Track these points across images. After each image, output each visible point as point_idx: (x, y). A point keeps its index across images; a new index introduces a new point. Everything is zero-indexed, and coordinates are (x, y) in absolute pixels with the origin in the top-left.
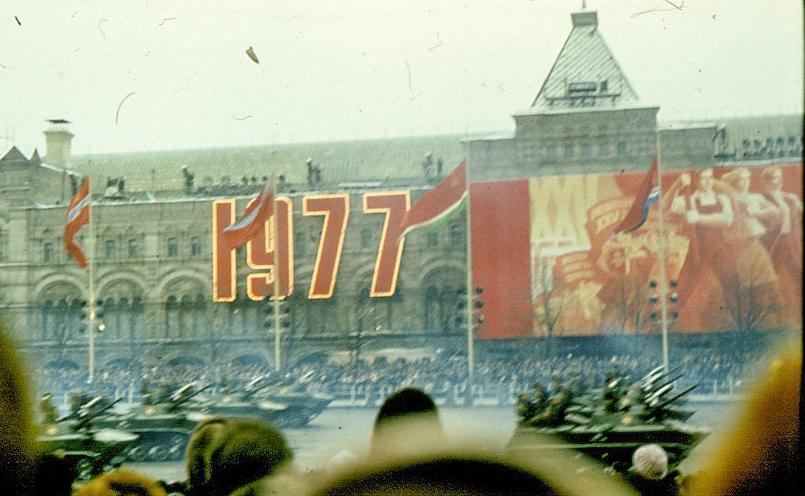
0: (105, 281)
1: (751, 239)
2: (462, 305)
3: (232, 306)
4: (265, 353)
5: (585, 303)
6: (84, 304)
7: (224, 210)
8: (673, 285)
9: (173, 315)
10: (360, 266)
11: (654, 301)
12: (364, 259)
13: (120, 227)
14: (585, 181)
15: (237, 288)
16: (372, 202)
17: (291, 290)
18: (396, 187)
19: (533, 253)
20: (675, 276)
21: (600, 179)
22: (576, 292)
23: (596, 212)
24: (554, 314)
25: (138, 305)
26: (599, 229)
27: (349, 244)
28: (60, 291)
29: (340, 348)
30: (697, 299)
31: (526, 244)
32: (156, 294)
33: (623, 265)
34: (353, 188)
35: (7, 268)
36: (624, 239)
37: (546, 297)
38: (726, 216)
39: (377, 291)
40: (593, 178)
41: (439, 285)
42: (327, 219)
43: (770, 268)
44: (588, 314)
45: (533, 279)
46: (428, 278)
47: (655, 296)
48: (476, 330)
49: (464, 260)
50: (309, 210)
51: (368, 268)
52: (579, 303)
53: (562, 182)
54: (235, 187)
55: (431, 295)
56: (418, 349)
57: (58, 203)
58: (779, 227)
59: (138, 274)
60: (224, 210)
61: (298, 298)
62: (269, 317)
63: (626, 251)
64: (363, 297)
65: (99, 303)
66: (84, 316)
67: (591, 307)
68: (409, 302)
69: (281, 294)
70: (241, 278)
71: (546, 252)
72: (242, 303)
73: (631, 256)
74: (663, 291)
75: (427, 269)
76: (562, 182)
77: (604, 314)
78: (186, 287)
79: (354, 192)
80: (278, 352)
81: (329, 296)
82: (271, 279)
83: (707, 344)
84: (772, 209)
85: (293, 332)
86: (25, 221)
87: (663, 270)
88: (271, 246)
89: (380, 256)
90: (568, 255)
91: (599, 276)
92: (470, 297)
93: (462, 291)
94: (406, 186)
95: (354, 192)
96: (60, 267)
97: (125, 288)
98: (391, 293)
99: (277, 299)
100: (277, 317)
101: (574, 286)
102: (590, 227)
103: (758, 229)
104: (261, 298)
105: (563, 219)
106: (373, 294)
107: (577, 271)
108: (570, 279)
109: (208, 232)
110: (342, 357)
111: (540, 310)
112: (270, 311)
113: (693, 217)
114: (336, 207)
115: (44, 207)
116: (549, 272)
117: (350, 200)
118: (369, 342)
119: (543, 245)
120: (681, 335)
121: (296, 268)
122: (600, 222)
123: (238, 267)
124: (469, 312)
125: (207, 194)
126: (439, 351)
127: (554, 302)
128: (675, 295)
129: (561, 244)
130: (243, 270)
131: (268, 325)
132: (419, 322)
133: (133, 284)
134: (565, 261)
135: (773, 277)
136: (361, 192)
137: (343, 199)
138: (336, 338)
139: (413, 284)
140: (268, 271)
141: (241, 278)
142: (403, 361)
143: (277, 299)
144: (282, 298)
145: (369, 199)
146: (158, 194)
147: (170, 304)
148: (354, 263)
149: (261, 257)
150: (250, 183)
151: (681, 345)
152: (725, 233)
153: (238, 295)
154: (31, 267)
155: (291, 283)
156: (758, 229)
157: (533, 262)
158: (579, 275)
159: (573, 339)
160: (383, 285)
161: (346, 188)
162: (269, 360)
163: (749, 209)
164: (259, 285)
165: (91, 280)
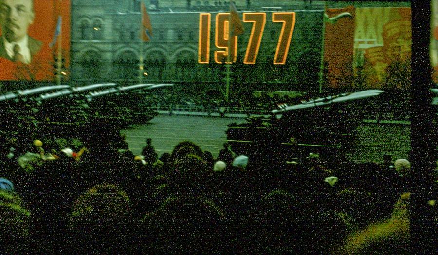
0: (149, 51)
2: (318, 70)
4: (220, 88)
6: (138, 62)
7: (205, 18)
9: (179, 69)
10: (269, 49)
12: (271, 46)
13: (155, 25)
14: (383, 11)
15: (210, 58)
16: (278, 17)
17: (235, 59)
18: (290, 9)
19: (355, 47)
21: (392, 11)
23: (387, 27)
25: (163, 64)
26: (389, 34)
28: (128, 55)
32: (172, 58)
34: (268, 9)
35: (101, 43)
36: (401, 42)
37: (359, 68)
40: (388, 9)
42: (254, 25)
44: (380, 78)
49: (320, 48)
50: (246, 20)
53: (371, 11)
54: (211, 7)
56: (295, 92)
57: (127, 12)
59: (165, 49)
60: (205, 18)
62: (224, 73)
65: (145, 62)
66: (138, 68)
67: (382, 76)
69: (230, 61)
70: (212, 52)
71: (361, 46)
72: (212, 64)
76: (371, 11)
77: (387, 79)
78: (186, 55)
79: (268, 11)
80: (228, 89)
81: (254, 63)
82: (226, 54)
86: (111, 21)
88: (226, 38)
89: (279, 44)
90: (372, 48)
92: (322, 67)
94: (293, 10)
95: (268, 11)
96: (127, 44)
97: (157, 55)
101: (373, 64)
102: (384, 35)
104: (221, 63)
105: (371, 30)
109: (198, 29)
110: (258, 94)
114: (259, 18)
115: (121, 13)
116: (362, 57)
117: (267, 15)
121: (239, 48)
123: (211, 47)
124: (321, 74)
125: (198, 10)
127: (363, 72)
129: (369, 43)
131: (225, 76)
133: (160, 53)
136: (272, 11)
137: (263, 15)
140: (224, 50)
144: (231, 63)
145: (276, 15)
146: (174, 9)
147: (178, 63)
148: (266, 47)
149: (222, 43)
150: (218, 5)
153: (210, 61)
154: (115, 43)
155: (236, 55)
157: (354, 51)
161: (264, 9)
162: (223, 91)
164: (221, 57)
165: (141, 50)
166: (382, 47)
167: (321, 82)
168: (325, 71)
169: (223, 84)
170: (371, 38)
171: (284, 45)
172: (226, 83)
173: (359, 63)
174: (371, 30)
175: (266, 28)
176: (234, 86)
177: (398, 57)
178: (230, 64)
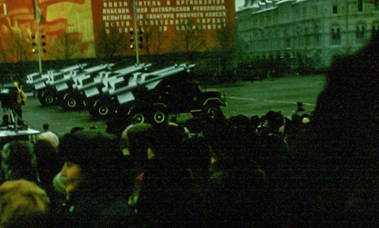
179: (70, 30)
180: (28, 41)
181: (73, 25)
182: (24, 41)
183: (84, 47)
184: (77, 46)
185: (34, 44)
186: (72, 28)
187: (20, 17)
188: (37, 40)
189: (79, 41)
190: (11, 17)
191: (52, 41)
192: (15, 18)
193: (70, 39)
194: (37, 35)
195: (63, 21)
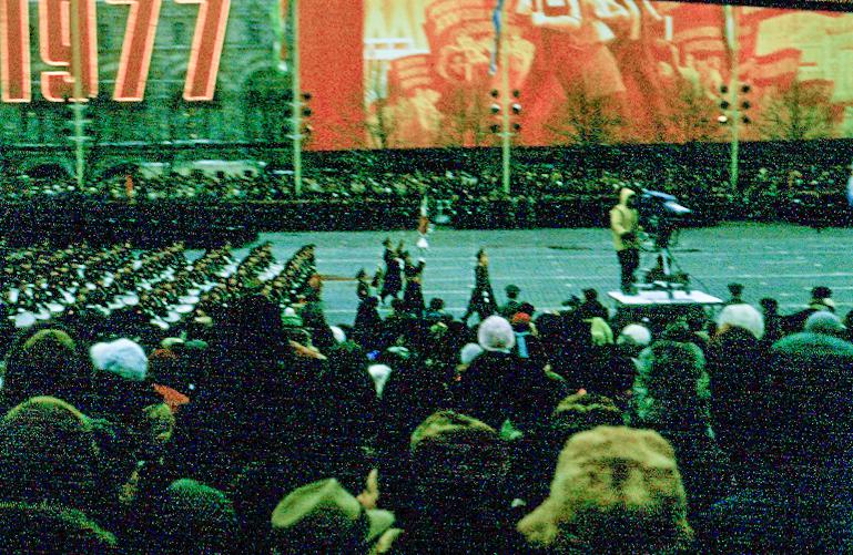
1: (600, 44)
2: (288, 113)
3: (24, 108)
4: (65, 163)
5: (421, 112)
8: (516, 94)
10: (172, 66)
11: (495, 111)
12: (176, 57)
17: (94, 94)
19: (367, 56)
20: (519, 85)
22: (413, 100)
23: (435, 11)
24: (388, 124)
26: (440, 27)
27: (161, 40)
29: (150, 157)
30: (539, 113)
31: (357, 45)
33: (463, 69)
36: (465, 43)
37: (380, 105)
38: (573, 20)
39: (193, 94)
41: (262, 89)
43: (617, 77)
44: (425, 124)
45: (366, 84)
46: (250, 83)
47: (497, 107)
48: (303, 143)
51: (183, 66)
52: (416, 113)
55: (253, 99)
58: (627, 33)
61: (103, 100)
63: (467, 55)
64: (176, 101)
67: (428, 118)
68: (231, 109)
70: (35, 76)
71: (380, 54)
72: (39, 104)
73: (473, 61)
74: (506, 101)
75: (249, 71)
77: (443, 124)
80: (81, 161)
81: (139, 99)
83: (550, 160)
84: (622, 12)
85: (99, 137)
87: (505, 76)
90: (403, 59)
91: (437, 83)
92: (297, 105)
93: (288, 96)
98: (208, 97)
99: (79, 102)
100: (79, 123)
101: (409, 94)
102: (429, 28)
103: (606, 34)
105: (400, 18)
106: (187, 97)
107: (417, 76)
108: (406, 85)
111: (373, 120)
112: (70, 115)
113: (540, 19)
116: (384, 79)
118: (184, 152)
119: (378, 46)
120: (521, 149)
121: (101, 64)
122: (438, 22)
124: (296, 121)
126: (263, 164)
127: (388, 112)
128: (517, 106)
129: (398, 46)
130: (38, 66)
131: (68, 132)
132: (240, 132)
134: (401, 65)
135: (620, 87)
138: (145, 148)
139: (231, 87)
141: (35, 76)
142: (220, 175)
143: (79, 102)
148: (165, 61)
151: (524, 160)
152: (572, 36)
153: (33, 96)
155: (95, 81)
156: (606, 34)
158: (417, 81)
159: (408, 153)
160: (199, 87)
162: (69, 169)
163: (599, 13)
166: (426, 56)
167: (297, 137)
168: (306, 113)
169: (69, 151)
170: (401, 35)
171: (206, 53)
172: (75, 147)
173: (378, 93)
174: (400, 18)
175: (161, 17)
176: (94, 154)
177: (461, 77)
178: (84, 103)
179: (805, 74)
180: (712, 97)
181: (813, 64)
182: (704, 98)
183: (833, 114)
184: (818, 112)
185: (725, 105)
186: (815, 68)
187: (699, 46)
188: (733, 96)
189: (824, 100)
190: (680, 46)
191: (766, 99)
192: (689, 48)
193: (799, 94)
194: (734, 85)
195: (794, 54)
